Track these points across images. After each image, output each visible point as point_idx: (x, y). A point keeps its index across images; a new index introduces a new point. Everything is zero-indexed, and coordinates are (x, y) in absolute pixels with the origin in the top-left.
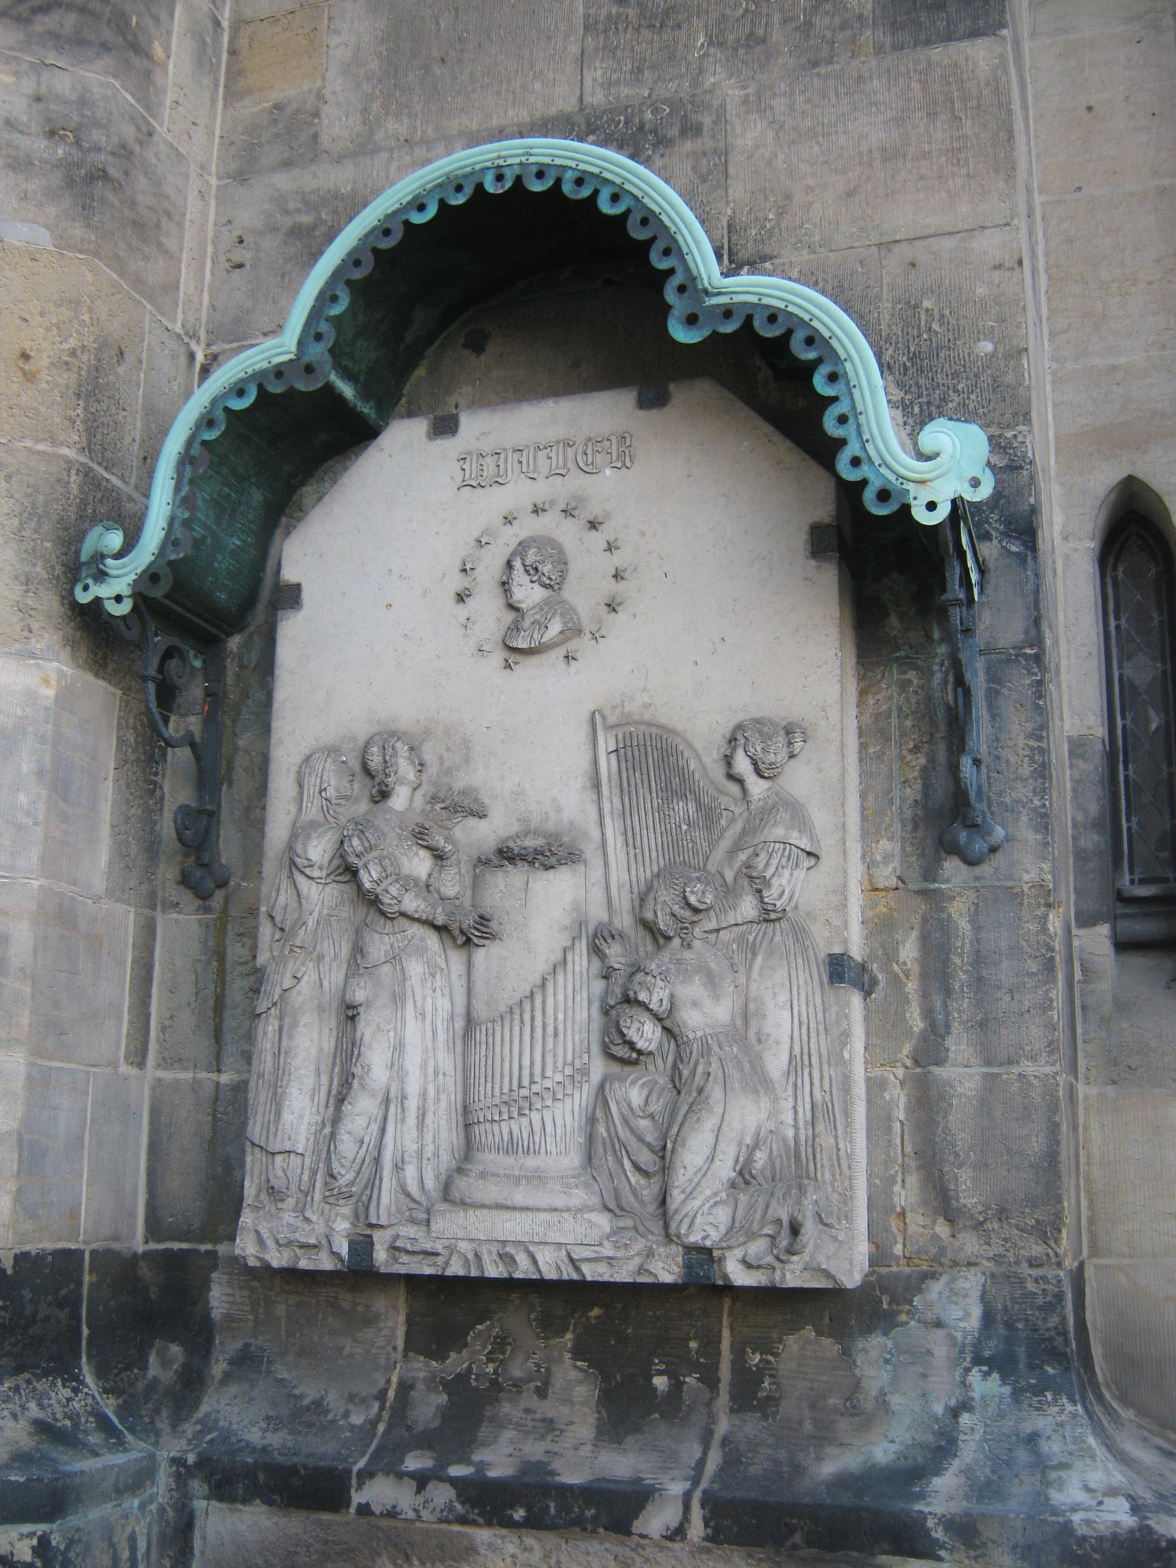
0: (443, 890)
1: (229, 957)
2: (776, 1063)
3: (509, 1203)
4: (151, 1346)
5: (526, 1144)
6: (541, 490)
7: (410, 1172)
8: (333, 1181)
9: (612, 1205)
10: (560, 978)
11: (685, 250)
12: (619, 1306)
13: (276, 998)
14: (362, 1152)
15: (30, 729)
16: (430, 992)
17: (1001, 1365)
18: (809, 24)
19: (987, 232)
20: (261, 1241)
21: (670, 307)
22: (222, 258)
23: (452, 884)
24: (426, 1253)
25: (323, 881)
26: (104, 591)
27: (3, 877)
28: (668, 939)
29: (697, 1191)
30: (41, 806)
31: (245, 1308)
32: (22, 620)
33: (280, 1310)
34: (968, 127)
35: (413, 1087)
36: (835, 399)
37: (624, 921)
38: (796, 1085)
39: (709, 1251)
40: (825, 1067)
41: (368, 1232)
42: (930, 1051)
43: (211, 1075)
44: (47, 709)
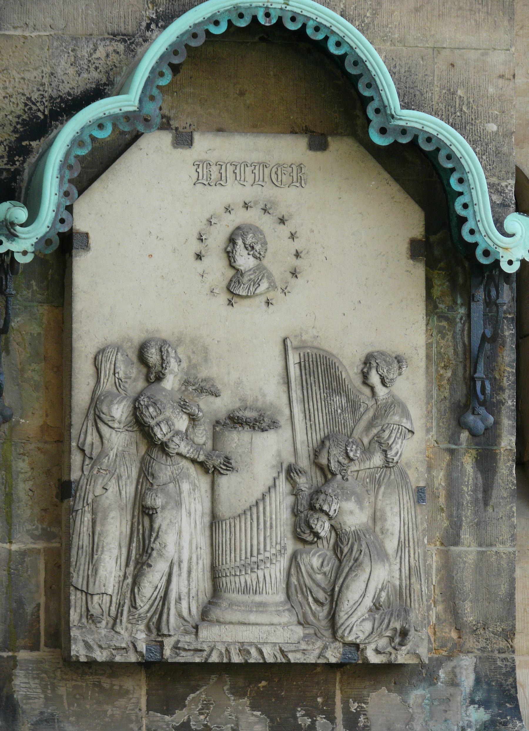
0: (196, 440)
1: (14, 468)
2: (391, 545)
3: (247, 621)
6: (249, 193)
7: (184, 604)
8: (134, 610)
10: (273, 495)
11: (381, 88)
12: (276, 680)
13: (90, 501)
14: (156, 593)
16: (193, 500)
23: (202, 436)
24: (196, 650)
26: (15, 247)
28: (334, 475)
29: (355, 613)
31: (38, 691)
33: (62, 691)
35: (185, 557)
36: (461, 194)
37: (304, 463)
38: (401, 558)
39: (357, 646)
40: (416, 548)
41: (160, 639)
42: (452, 538)
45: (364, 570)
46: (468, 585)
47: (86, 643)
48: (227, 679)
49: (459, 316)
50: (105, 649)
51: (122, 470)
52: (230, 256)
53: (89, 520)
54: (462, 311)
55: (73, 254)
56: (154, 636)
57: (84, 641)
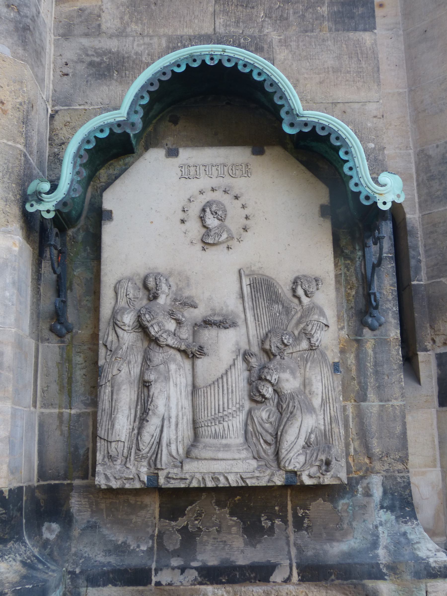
1: (74, 361)
2: (317, 402)
3: (216, 458)
4: (43, 525)
5: (222, 435)
6: (215, 182)
7: (173, 447)
8: (139, 452)
9: (257, 457)
10: (233, 370)
11: (289, 98)
12: (247, 495)
13: (110, 378)
14: (153, 440)
15: (9, 264)
16: (179, 376)
17: (391, 508)
18: (303, 16)
19: (371, 104)
20: (107, 478)
21: (283, 119)
22: (58, 70)
23: (185, 333)
24: (182, 479)
25: (130, 331)
26: (42, 207)
27: (1, 327)
28: (275, 356)
29: (292, 450)
30: (15, 297)
31: (87, 506)
32: (4, 217)
33: (103, 506)
34: (363, 64)
35: (173, 414)
36: (347, 161)
37: (255, 349)
38: (324, 410)
39: (295, 473)
40: (335, 403)
41: (156, 472)
43: (67, 410)
44: (15, 256)
45: (297, 420)
46: (374, 428)
47: (106, 476)
48: (214, 496)
49: (358, 257)
50: (119, 479)
51: (131, 357)
52: (202, 219)
53: (109, 391)
54: (360, 253)
55: (102, 224)
56: (152, 470)
57: (104, 474)
